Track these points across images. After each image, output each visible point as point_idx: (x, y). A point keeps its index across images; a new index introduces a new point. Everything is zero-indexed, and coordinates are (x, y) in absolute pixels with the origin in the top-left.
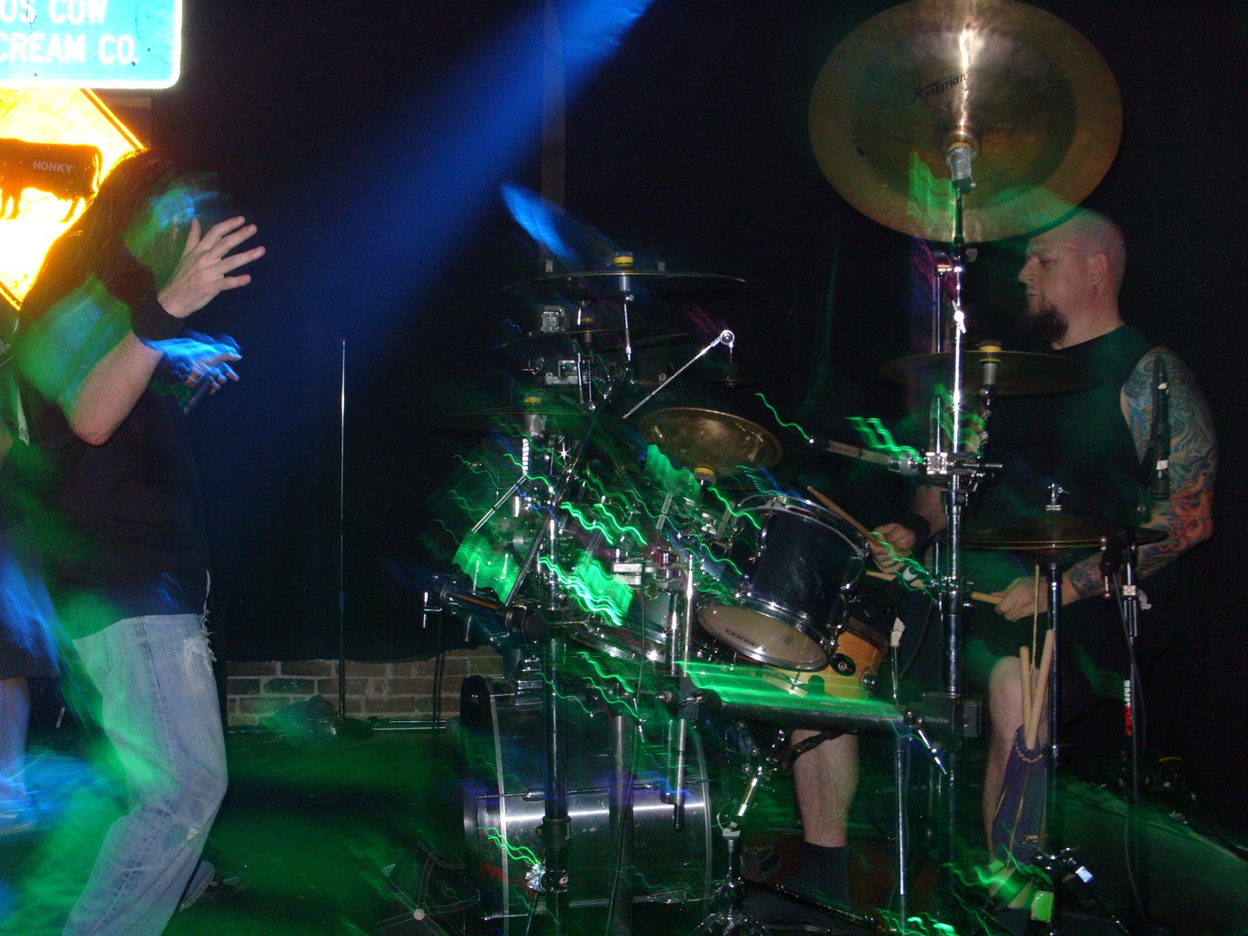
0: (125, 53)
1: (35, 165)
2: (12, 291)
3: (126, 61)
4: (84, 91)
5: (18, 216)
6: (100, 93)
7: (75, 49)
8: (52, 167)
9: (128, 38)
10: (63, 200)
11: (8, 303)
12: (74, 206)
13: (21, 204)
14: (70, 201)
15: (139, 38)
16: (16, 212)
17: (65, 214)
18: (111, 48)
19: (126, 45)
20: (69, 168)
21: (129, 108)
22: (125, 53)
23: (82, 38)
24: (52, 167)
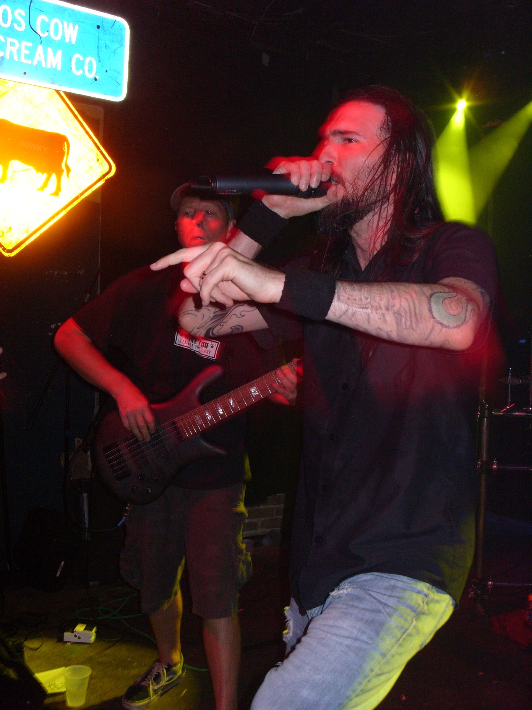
0: (90, 71)
3: (92, 76)
4: (58, 92)
7: (54, 60)
9: (91, 60)
10: (40, 174)
12: (48, 179)
13: (9, 172)
14: (45, 175)
15: (100, 61)
16: (4, 178)
18: (80, 65)
19: (90, 63)
21: (89, 109)
22: (90, 71)
23: (60, 52)
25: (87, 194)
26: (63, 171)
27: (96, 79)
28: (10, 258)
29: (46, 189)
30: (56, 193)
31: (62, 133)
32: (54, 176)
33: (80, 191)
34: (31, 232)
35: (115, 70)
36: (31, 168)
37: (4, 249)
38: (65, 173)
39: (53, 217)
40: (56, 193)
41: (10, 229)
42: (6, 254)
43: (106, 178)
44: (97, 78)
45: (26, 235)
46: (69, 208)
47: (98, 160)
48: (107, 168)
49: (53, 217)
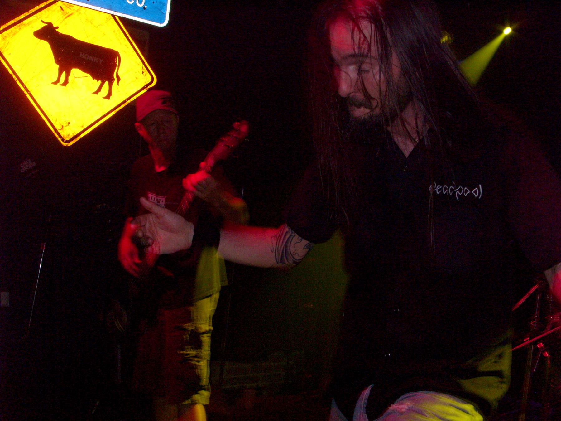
1: (81, 55)
2: (59, 131)
4: (113, 16)
5: (68, 85)
6: (121, 18)
8: (91, 58)
10: (95, 80)
11: (57, 138)
13: (70, 78)
14: (100, 82)
16: (66, 83)
17: (96, 89)
20: (101, 61)
24: (91, 58)
25: (132, 99)
26: (114, 79)
27: (144, 8)
28: (67, 147)
29: (99, 93)
30: (108, 97)
31: (115, 49)
32: (107, 83)
33: (127, 97)
34: (85, 127)
35: (160, 2)
36: (88, 75)
37: (63, 140)
38: (116, 81)
39: (104, 116)
40: (108, 97)
41: (69, 123)
42: (64, 144)
43: (149, 87)
44: (146, 7)
45: (82, 129)
46: (117, 110)
47: (143, 73)
48: (149, 79)
49: (104, 116)
